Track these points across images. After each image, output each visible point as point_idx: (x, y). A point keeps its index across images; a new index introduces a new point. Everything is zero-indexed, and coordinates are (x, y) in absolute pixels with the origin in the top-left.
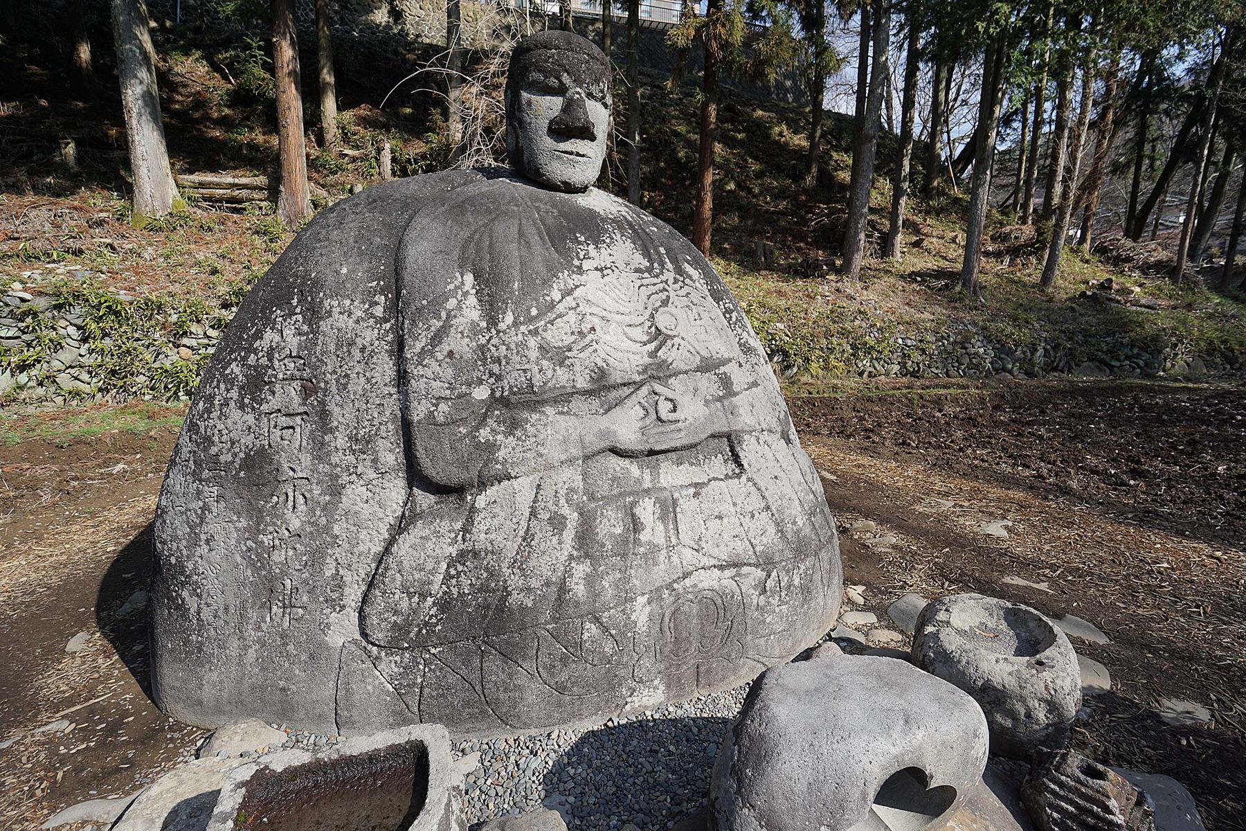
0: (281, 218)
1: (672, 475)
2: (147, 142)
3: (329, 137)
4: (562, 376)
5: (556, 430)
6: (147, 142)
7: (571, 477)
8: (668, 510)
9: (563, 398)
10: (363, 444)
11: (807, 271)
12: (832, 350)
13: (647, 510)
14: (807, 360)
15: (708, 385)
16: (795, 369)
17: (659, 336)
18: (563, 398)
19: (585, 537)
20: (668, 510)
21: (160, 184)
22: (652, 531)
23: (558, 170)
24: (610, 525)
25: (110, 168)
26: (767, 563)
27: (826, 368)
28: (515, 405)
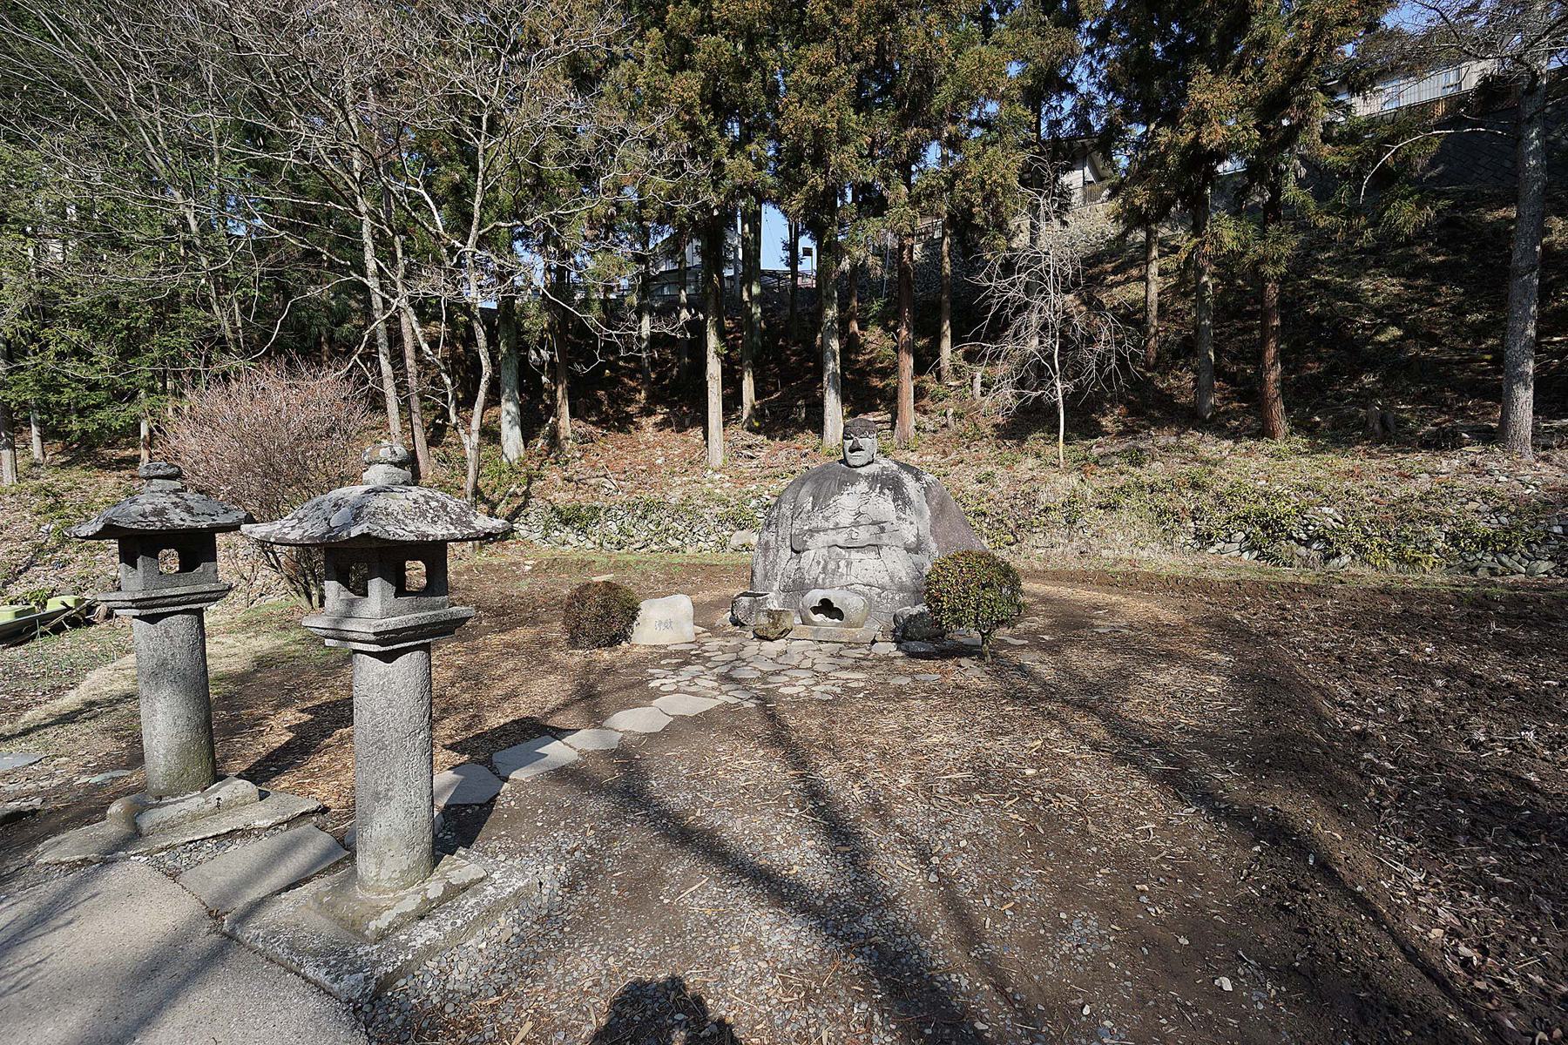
0: (895, 441)
1: (855, 555)
2: (833, 406)
3: (944, 373)
4: (826, 525)
5: (821, 539)
6: (833, 406)
7: (825, 551)
8: (849, 564)
9: (825, 530)
10: (784, 540)
11: (1442, 442)
12: (1407, 539)
13: (843, 563)
14: (1358, 548)
15: (875, 529)
16: (1346, 559)
17: (859, 514)
18: (825, 530)
19: (824, 568)
20: (849, 564)
21: (836, 428)
22: (843, 570)
23: (851, 462)
24: (832, 566)
25: (816, 423)
26: (883, 588)
27: (1401, 559)
28: (813, 532)
